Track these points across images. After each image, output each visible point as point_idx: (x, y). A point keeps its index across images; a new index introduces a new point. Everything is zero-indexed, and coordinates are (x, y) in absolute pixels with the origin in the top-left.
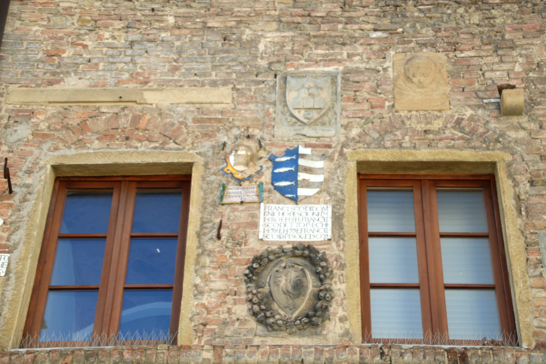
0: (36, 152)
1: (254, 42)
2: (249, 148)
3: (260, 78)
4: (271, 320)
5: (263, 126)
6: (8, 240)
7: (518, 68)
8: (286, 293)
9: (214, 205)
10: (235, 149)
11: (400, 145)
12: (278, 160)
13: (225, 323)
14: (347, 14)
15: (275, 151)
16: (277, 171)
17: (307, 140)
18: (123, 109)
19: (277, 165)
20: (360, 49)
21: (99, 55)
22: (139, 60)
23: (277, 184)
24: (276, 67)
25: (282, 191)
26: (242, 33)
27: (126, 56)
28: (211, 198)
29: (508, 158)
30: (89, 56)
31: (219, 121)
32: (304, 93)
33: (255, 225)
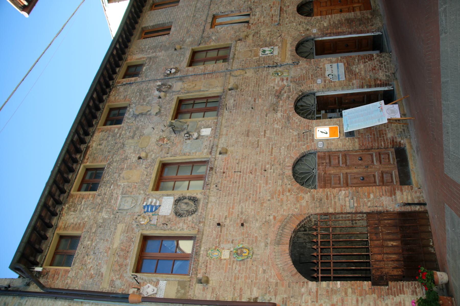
0: (126, 278)
1: (104, 220)
2: (140, 218)
3: (117, 217)
4: (195, 210)
5: (134, 215)
6: (155, 282)
7: (134, 155)
8: (187, 206)
9: (156, 227)
10: (139, 222)
11: (149, 181)
12: (146, 211)
13: (193, 222)
14: (102, 195)
15: (143, 212)
16: (149, 211)
17: (141, 204)
18: (117, 254)
19: (148, 211)
20: (116, 191)
21: (96, 263)
22: (101, 250)
23: (154, 211)
24: (114, 212)
25: (156, 209)
26: (100, 222)
27: (98, 255)
28: (154, 228)
29: (160, 158)
30: (95, 266)
31: (129, 227)
32: (126, 204)
33: (165, 216)
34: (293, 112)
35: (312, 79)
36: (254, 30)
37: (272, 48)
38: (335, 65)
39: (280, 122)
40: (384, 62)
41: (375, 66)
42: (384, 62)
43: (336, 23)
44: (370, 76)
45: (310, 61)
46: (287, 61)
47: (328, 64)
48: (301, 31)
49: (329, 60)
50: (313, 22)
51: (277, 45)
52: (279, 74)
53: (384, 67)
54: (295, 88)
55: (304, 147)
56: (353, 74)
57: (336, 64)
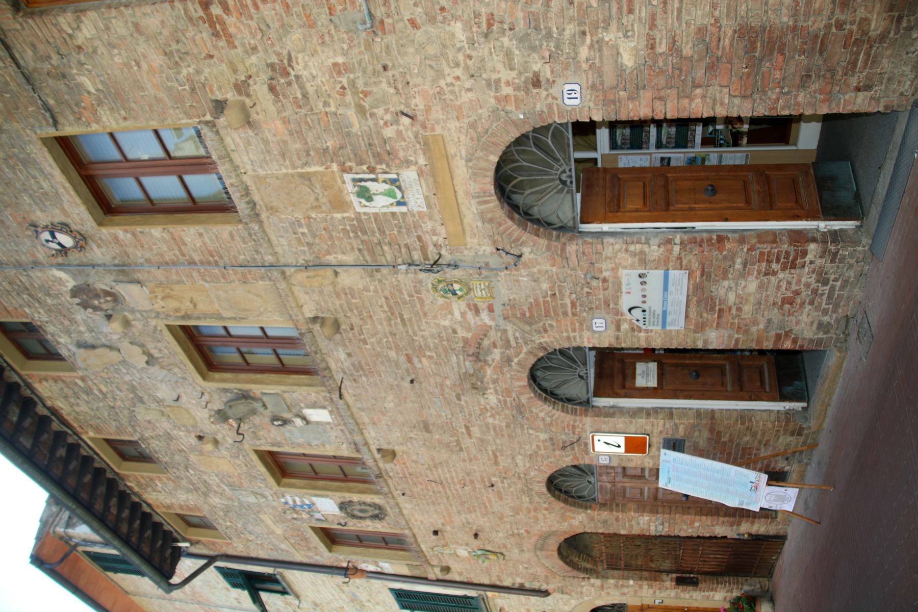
34: (528, 396)
35: (574, 314)
36: (254, 49)
37: (393, 182)
38: (655, 276)
39: (499, 414)
40: (836, 280)
41: (797, 293)
42: (836, 280)
43: (687, 51)
44: (769, 321)
45: (563, 250)
46: (471, 241)
47: (632, 267)
48: (507, 90)
49: (634, 254)
50: (562, 31)
51: (407, 163)
52: (459, 293)
53: (825, 297)
54: (524, 338)
55: (567, 459)
56: (712, 309)
57: (660, 273)
